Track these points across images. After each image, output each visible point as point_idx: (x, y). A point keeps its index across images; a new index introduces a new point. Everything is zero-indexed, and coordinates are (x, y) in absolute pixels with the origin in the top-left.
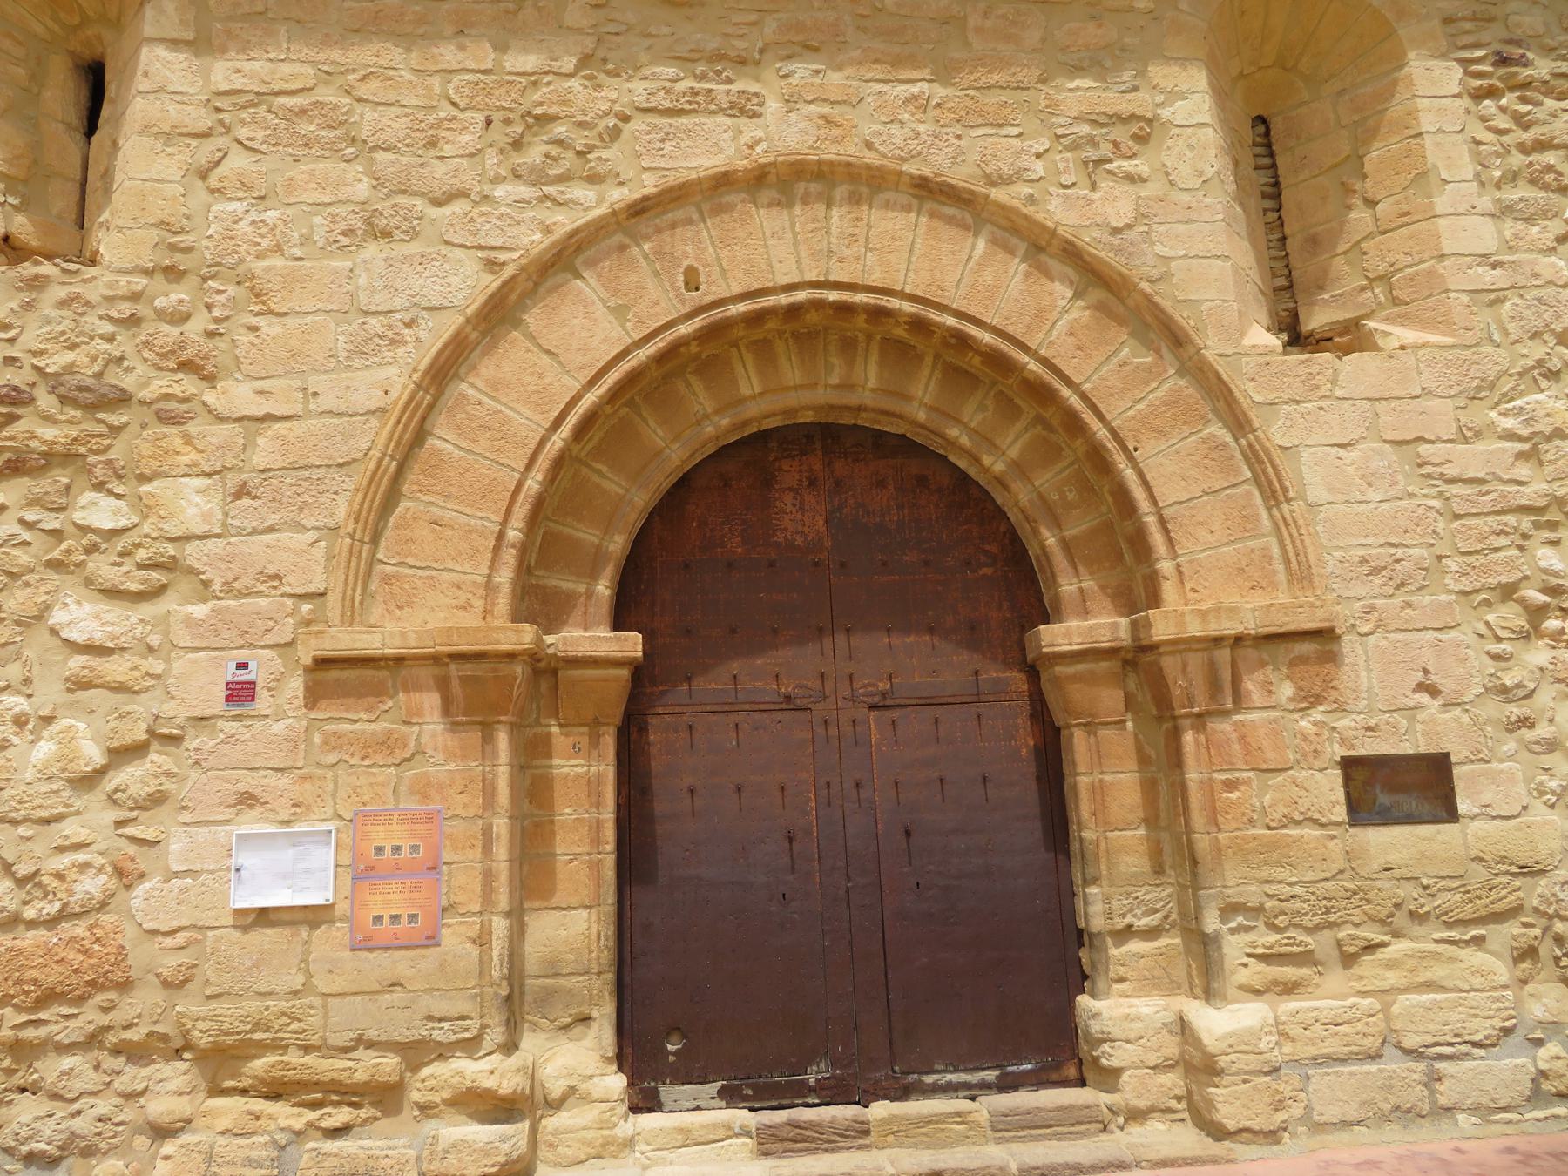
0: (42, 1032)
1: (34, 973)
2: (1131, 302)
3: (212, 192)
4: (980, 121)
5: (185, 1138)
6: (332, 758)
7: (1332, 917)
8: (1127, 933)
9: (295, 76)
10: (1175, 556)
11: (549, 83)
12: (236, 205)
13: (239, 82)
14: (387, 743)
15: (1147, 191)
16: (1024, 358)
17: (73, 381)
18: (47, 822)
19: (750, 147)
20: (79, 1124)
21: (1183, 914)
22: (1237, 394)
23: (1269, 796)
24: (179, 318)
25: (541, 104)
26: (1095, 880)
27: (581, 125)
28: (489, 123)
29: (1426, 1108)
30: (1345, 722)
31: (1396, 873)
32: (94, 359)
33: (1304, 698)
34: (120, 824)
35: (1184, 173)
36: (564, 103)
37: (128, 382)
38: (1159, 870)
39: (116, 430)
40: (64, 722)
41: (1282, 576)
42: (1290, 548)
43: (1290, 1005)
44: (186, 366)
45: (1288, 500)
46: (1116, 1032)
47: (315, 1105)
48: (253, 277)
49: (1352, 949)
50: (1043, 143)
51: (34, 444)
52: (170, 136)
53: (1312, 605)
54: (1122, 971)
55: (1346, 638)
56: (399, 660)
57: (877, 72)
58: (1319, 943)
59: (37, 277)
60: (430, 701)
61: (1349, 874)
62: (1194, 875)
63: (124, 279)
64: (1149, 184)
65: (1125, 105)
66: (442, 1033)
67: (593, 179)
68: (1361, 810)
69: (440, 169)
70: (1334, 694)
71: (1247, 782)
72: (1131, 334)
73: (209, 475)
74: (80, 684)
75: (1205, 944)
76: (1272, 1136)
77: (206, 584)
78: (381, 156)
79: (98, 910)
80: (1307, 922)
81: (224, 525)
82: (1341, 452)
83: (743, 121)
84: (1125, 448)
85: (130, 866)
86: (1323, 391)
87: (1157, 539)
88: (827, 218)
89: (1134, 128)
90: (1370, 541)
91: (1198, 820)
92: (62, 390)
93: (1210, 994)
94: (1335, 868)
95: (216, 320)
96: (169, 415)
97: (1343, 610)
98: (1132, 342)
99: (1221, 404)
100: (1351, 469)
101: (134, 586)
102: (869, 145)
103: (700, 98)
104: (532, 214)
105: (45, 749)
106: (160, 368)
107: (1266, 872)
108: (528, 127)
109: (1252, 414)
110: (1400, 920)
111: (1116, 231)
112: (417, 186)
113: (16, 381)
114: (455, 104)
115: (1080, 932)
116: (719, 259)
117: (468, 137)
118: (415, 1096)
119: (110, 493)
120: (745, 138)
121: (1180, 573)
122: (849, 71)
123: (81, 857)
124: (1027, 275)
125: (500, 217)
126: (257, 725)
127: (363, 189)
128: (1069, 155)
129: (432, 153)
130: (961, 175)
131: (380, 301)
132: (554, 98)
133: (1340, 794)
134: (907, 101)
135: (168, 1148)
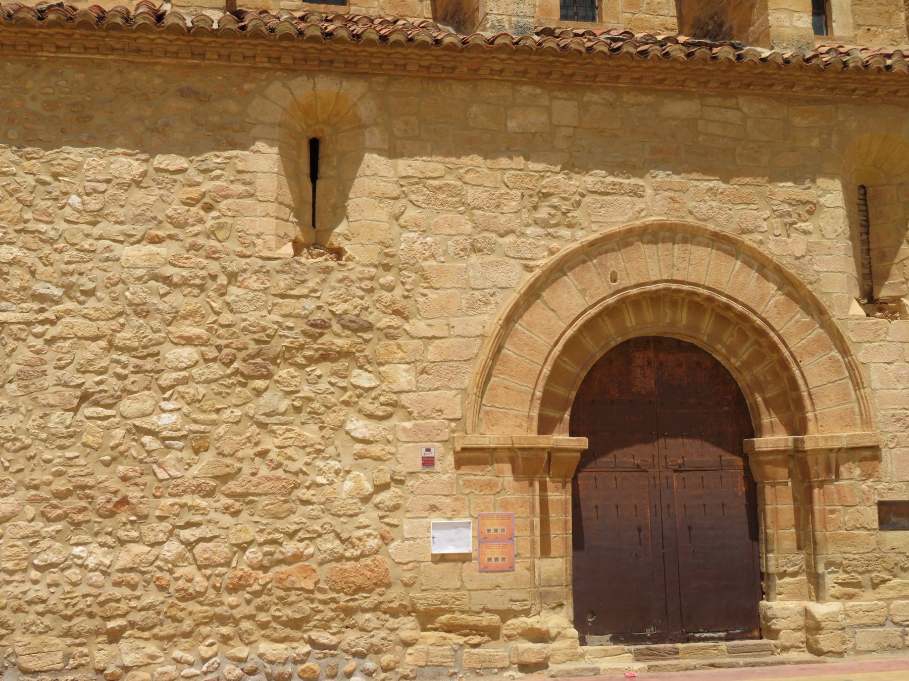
0: (356, 603)
1: (353, 579)
2: (802, 293)
3: (402, 227)
4: (740, 201)
5: (416, 647)
6: (467, 491)
7: (870, 568)
8: (783, 575)
9: (435, 170)
10: (814, 410)
11: (549, 177)
12: (412, 235)
13: (410, 172)
14: (489, 485)
15: (813, 238)
16: (755, 318)
17: (347, 317)
18: (351, 516)
19: (639, 213)
20: (374, 640)
21: (808, 566)
22: (845, 338)
23: (847, 517)
24: (390, 289)
25: (545, 187)
26: (772, 551)
27: (564, 199)
28: (523, 196)
29: (901, 646)
30: (880, 486)
31: (897, 551)
32: (355, 307)
33: (864, 475)
34: (381, 518)
35: (829, 231)
36: (556, 187)
37: (371, 318)
38: (799, 548)
39: (367, 341)
40: (355, 473)
41: (859, 421)
42: (863, 409)
43: (850, 603)
44: (397, 312)
45: (864, 388)
46: (779, 615)
47: (465, 635)
48: (423, 270)
49: (877, 581)
50: (767, 213)
51: (333, 347)
52: (381, 198)
53: (871, 436)
54: (781, 590)
55: (883, 450)
56: (495, 449)
57: (695, 175)
58: (864, 579)
59: (328, 267)
60: (508, 467)
61: (877, 550)
62: (815, 549)
63: (366, 269)
64: (813, 235)
65: (804, 197)
66: (516, 606)
67: (570, 226)
68: (885, 523)
69: (503, 219)
70: (877, 474)
71: (839, 511)
72: (802, 308)
73: (408, 363)
74: (359, 456)
75: (818, 578)
76: (840, 654)
77: (410, 413)
78: (476, 212)
79: (375, 554)
80: (859, 570)
81: (417, 387)
82: (888, 366)
83: (635, 198)
84: (796, 361)
85: (388, 535)
86: (881, 338)
87: (807, 403)
88: (673, 249)
89: (808, 207)
90: (896, 407)
91: (818, 526)
92: (343, 322)
93: (818, 599)
94: (872, 547)
95: (407, 290)
96: (390, 335)
97: (885, 438)
98: (802, 311)
99: (838, 342)
100: (891, 374)
101: (380, 413)
102: (691, 213)
103: (617, 187)
104: (543, 242)
105: (348, 485)
106: (384, 313)
107: (844, 549)
108: (540, 198)
109: (851, 348)
110: (897, 570)
111: (797, 258)
112: (493, 227)
113: (323, 317)
114: (507, 186)
115: (762, 574)
116: (626, 268)
117: (514, 203)
118: (505, 632)
119: (366, 370)
120: (637, 208)
121: (816, 418)
122: (683, 175)
123: (367, 531)
124: (758, 279)
125: (530, 244)
126: (436, 476)
127: (468, 228)
128: (778, 220)
129: (499, 210)
130: (729, 230)
131: (479, 284)
132: (551, 184)
133: (876, 517)
134: (708, 190)
135: (410, 650)
